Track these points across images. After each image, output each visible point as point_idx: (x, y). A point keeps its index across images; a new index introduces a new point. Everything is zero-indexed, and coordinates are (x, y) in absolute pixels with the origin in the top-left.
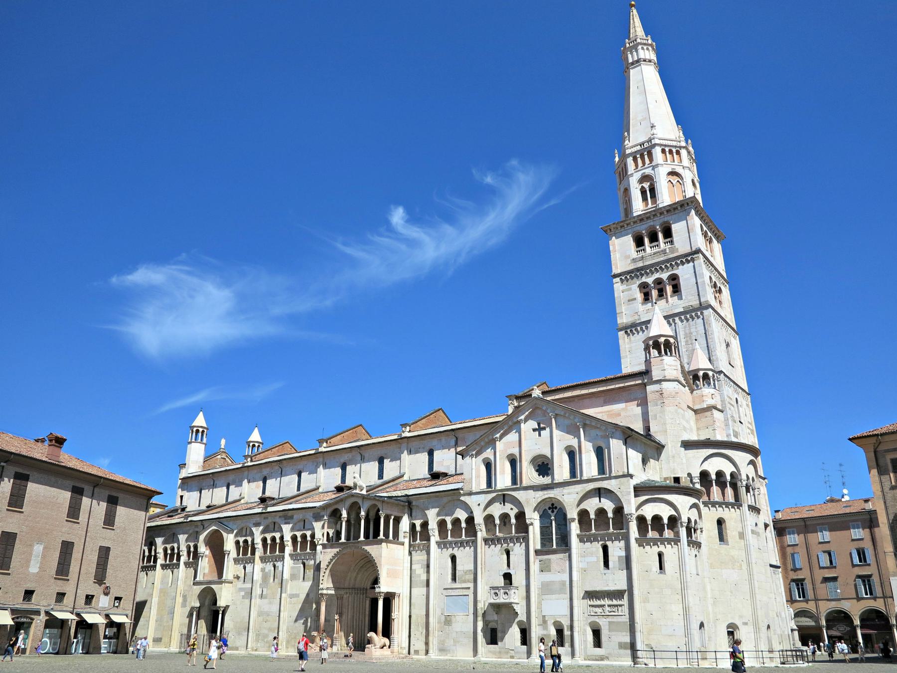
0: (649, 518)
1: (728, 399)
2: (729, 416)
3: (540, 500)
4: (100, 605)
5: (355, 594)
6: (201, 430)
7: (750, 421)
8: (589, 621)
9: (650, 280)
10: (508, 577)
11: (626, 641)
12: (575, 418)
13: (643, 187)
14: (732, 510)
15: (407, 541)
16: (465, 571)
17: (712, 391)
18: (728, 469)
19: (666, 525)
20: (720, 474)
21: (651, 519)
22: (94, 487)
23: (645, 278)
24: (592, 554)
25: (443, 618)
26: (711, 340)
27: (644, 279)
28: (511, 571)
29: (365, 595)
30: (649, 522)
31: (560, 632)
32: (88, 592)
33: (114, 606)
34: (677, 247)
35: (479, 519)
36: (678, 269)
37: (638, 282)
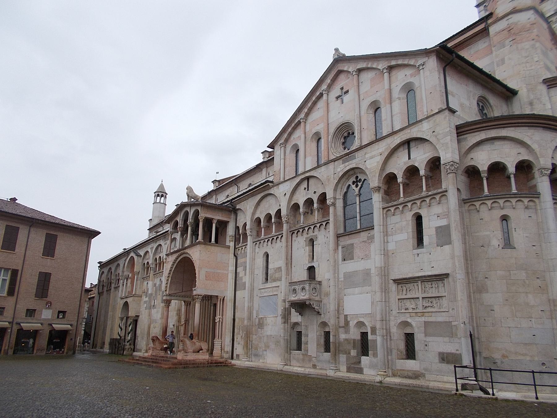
3: (341, 174)
4: (43, 317)
5: (206, 301)
6: (160, 194)
8: (399, 321)
10: (311, 269)
11: (449, 351)
12: (378, 64)
15: (232, 244)
16: (275, 269)
19: (512, 176)
21: (486, 169)
22: (30, 227)
24: (402, 230)
25: (257, 320)
28: (315, 264)
29: (210, 301)
30: (484, 175)
31: (364, 335)
32: (28, 307)
33: (58, 317)
35: (284, 213)
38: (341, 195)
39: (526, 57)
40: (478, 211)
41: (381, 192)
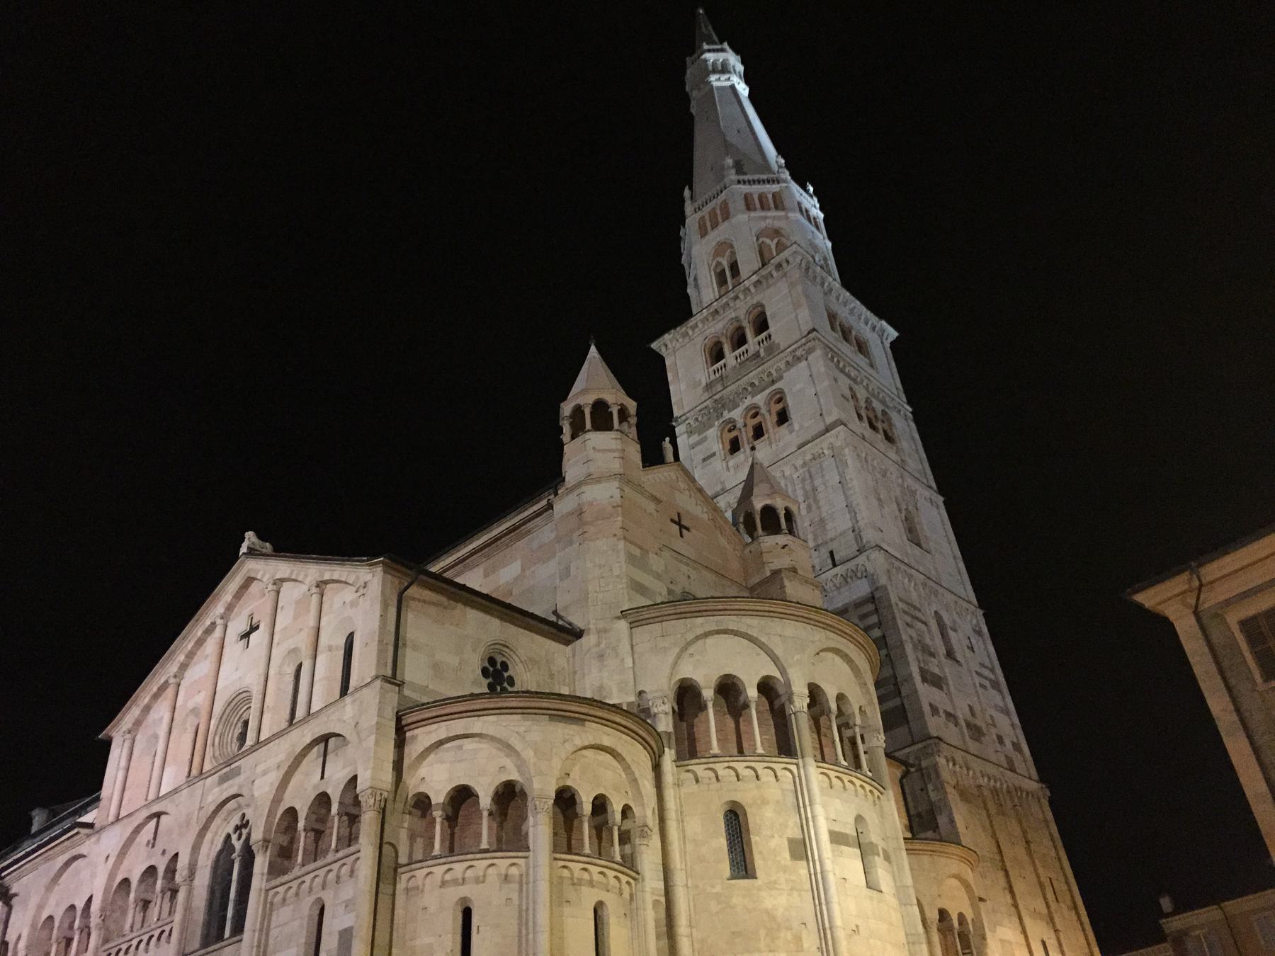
0: (439, 796)
1: (901, 605)
2: (904, 637)
7: (987, 663)
9: (737, 414)
13: (719, 263)
14: (767, 776)
17: (781, 539)
18: (750, 673)
20: (728, 689)
23: (729, 412)
26: (851, 492)
27: (727, 415)
34: (776, 342)
36: (781, 378)
37: (716, 423)
38: (208, 859)
39: (600, 567)
40: (422, 891)
41: (268, 853)
